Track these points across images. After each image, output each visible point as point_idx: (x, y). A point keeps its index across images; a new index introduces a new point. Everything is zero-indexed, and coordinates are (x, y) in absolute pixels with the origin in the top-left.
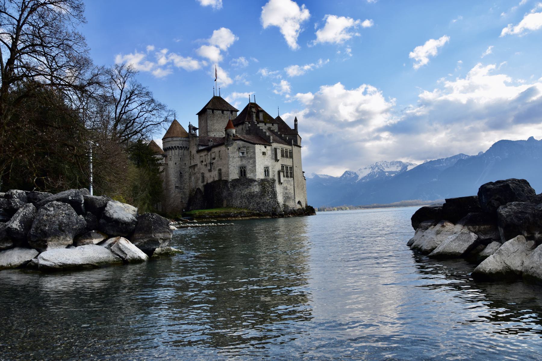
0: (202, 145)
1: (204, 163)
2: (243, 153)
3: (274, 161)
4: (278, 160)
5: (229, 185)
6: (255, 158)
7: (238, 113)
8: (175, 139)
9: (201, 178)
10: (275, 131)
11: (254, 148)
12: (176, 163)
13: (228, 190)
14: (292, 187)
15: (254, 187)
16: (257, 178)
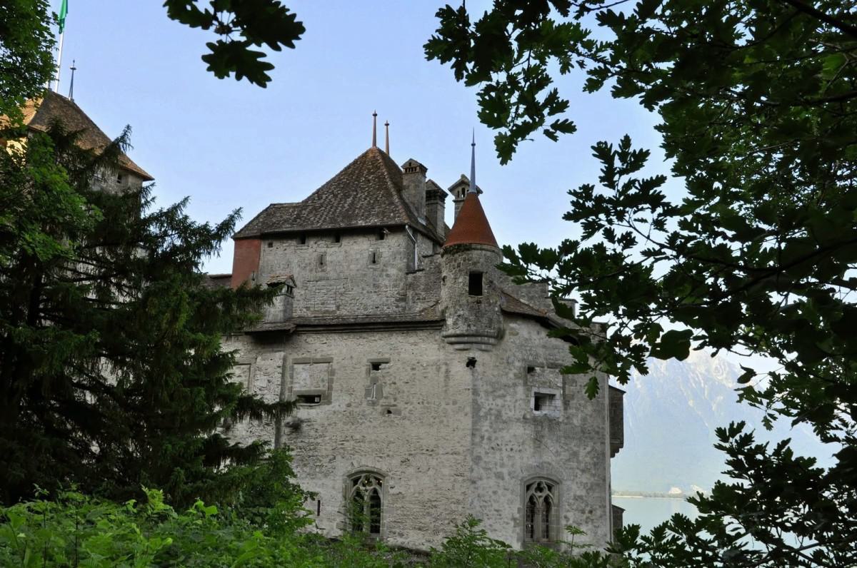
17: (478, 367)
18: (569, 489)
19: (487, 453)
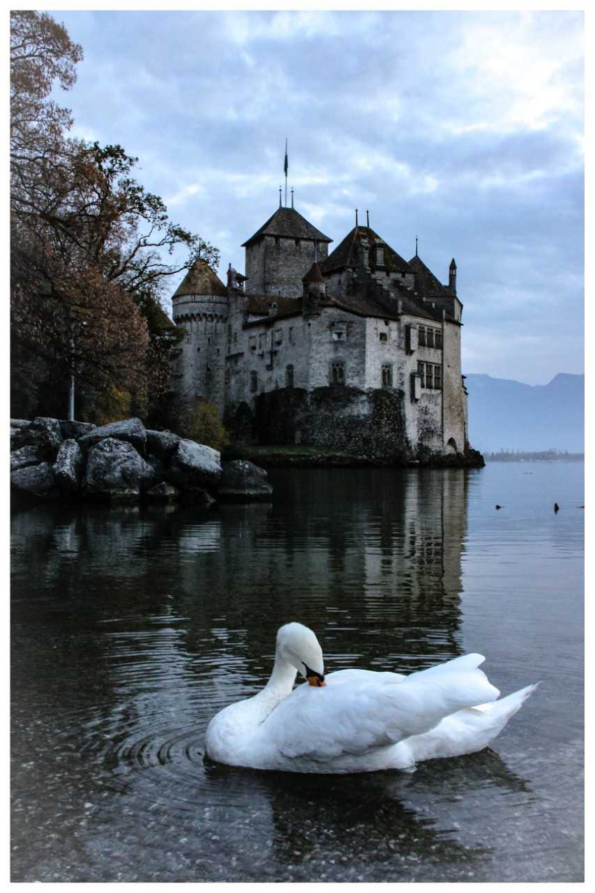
0: (255, 314)
1: (258, 352)
2: (339, 335)
3: (402, 353)
5: (308, 400)
6: (363, 346)
7: (331, 248)
8: (198, 298)
9: (250, 382)
10: (409, 289)
11: (364, 326)
12: (199, 349)
13: (307, 409)
14: (438, 409)
16: (367, 386)
17: (312, 326)
18: (349, 365)
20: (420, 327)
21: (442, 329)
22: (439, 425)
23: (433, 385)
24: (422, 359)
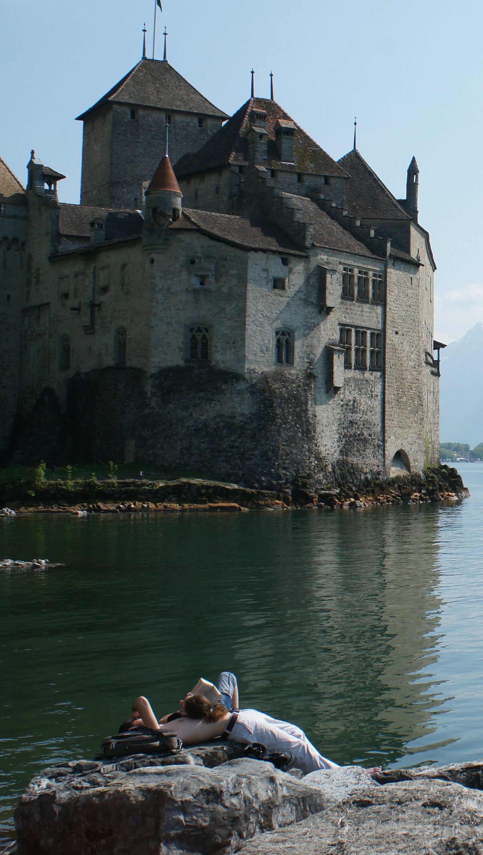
3: (311, 310)
4: (330, 309)
5: (148, 388)
11: (244, 265)
14: (377, 404)
15: (237, 399)
19: (161, 311)
20: (345, 269)
21: (385, 272)
22: (379, 429)
23: (368, 364)
24: (348, 321)
